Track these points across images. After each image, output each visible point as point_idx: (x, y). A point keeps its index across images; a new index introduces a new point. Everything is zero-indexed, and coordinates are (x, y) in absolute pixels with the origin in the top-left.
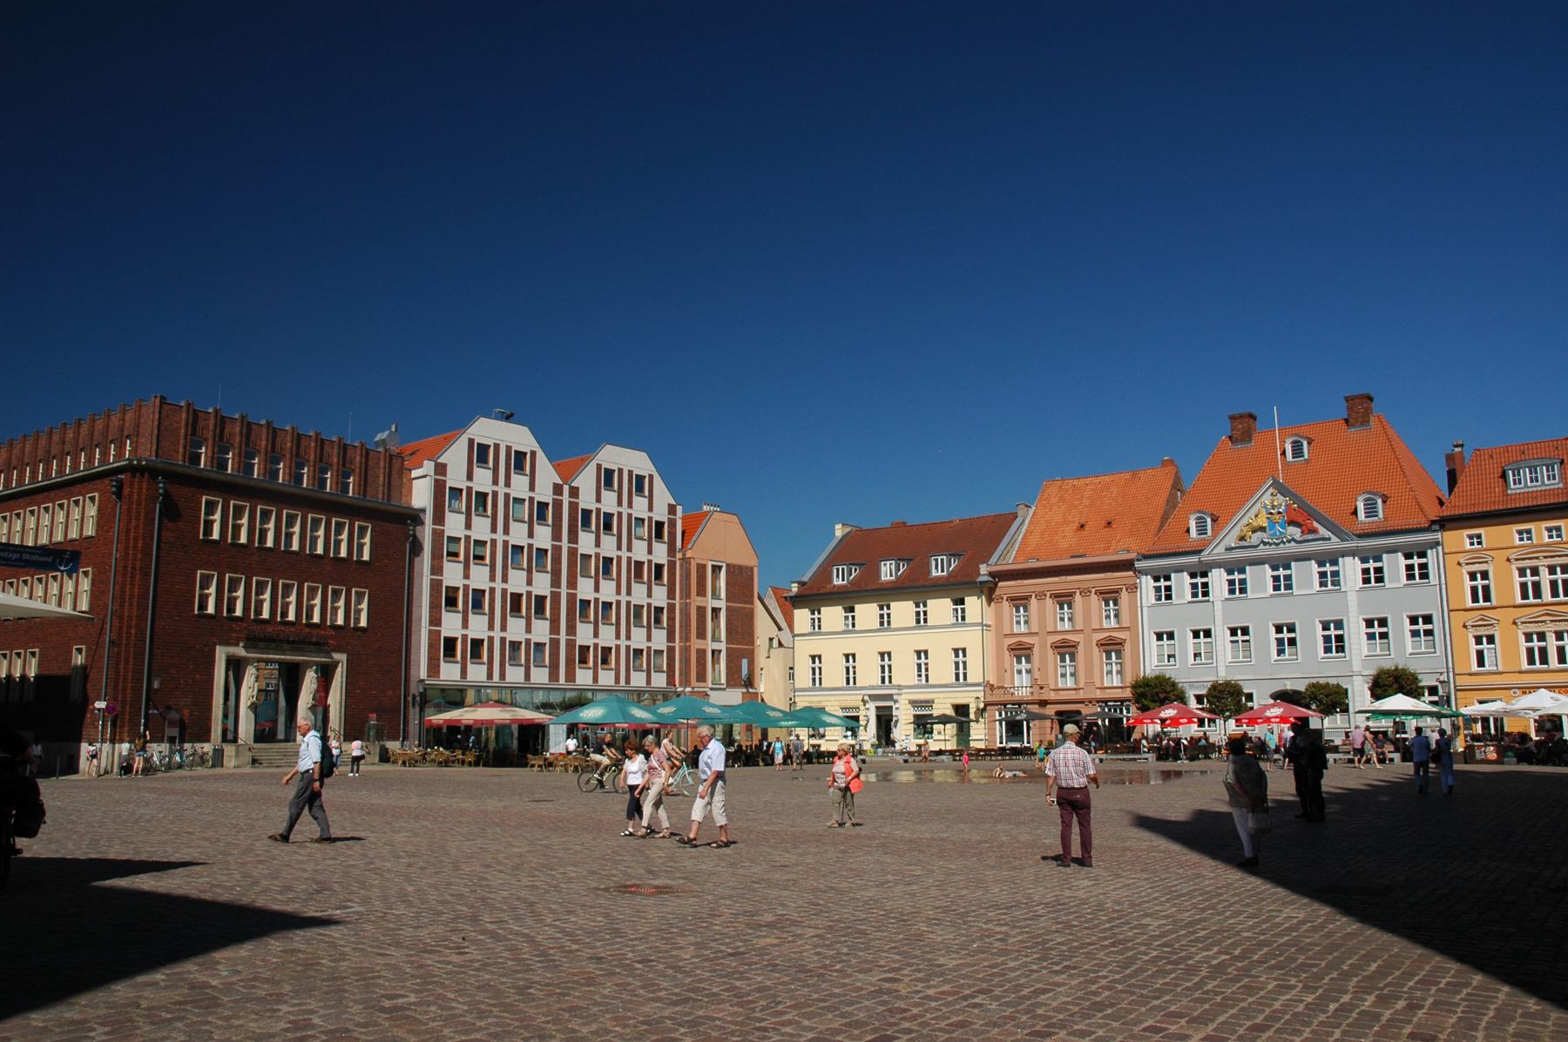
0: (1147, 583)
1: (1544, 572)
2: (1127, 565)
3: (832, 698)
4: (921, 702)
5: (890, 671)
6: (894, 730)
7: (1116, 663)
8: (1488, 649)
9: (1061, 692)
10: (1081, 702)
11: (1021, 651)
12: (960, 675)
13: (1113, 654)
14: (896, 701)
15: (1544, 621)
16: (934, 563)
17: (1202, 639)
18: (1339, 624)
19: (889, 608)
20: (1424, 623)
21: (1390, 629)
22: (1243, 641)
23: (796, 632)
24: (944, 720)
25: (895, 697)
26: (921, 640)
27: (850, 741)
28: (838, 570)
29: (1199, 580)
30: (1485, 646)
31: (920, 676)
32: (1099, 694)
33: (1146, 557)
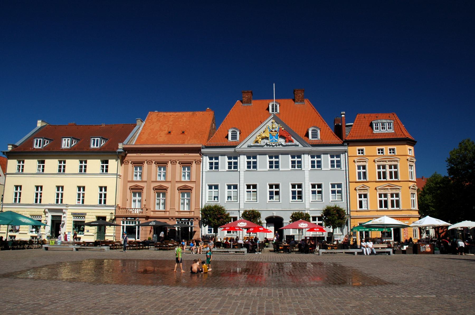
0: (206, 160)
1: (387, 167)
2: (197, 150)
3: (26, 210)
4: (79, 214)
5: (20, 196)
6: (62, 229)
7: (187, 199)
8: (364, 200)
9: (157, 213)
10: (167, 218)
11: (137, 190)
12: (103, 199)
13: (137, 194)
14: (64, 213)
15: (387, 189)
16: (92, 141)
17: (232, 190)
18: (300, 186)
19: (65, 162)
20: (318, 188)
21: (323, 189)
22: (253, 192)
23: (8, 172)
24: (90, 224)
25: (64, 211)
26: (82, 180)
27: (34, 234)
28: (37, 140)
29: (233, 161)
30: (363, 199)
31: (79, 200)
32: (177, 215)
33: (207, 147)
